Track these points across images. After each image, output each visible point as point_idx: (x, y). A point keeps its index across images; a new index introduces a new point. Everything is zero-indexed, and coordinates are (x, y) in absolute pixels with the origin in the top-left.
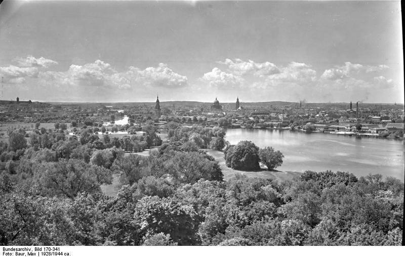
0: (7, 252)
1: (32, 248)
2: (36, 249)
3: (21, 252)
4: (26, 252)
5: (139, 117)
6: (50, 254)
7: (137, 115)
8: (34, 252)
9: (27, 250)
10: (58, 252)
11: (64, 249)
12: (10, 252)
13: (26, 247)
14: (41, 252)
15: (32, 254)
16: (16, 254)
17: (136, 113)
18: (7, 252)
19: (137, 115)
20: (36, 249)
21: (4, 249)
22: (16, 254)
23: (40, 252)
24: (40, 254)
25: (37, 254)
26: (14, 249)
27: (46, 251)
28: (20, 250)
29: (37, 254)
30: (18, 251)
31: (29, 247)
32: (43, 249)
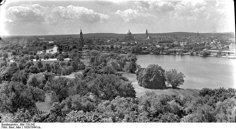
0: (4, 126)
1: (19, 124)
2: (21, 125)
3: (13, 126)
4: (15, 126)
5: (66, 46)
6: (29, 127)
7: (64, 45)
8: (20, 126)
9: (16, 125)
10: (34, 126)
11: (37, 124)
12: (6, 126)
13: (15, 123)
14: (24, 126)
15: (19, 127)
16: (10, 127)
17: (63, 44)
18: (4, 126)
19: (64, 45)
20: (21, 125)
21: (2, 124)
22: (10, 127)
23: (24, 126)
24: (24, 127)
25: (22, 127)
26: (8, 125)
27: (27, 126)
28: (12, 125)
29: (22, 127)
30: (10, 126)
31: (17, 123)
32: (25, 125)
